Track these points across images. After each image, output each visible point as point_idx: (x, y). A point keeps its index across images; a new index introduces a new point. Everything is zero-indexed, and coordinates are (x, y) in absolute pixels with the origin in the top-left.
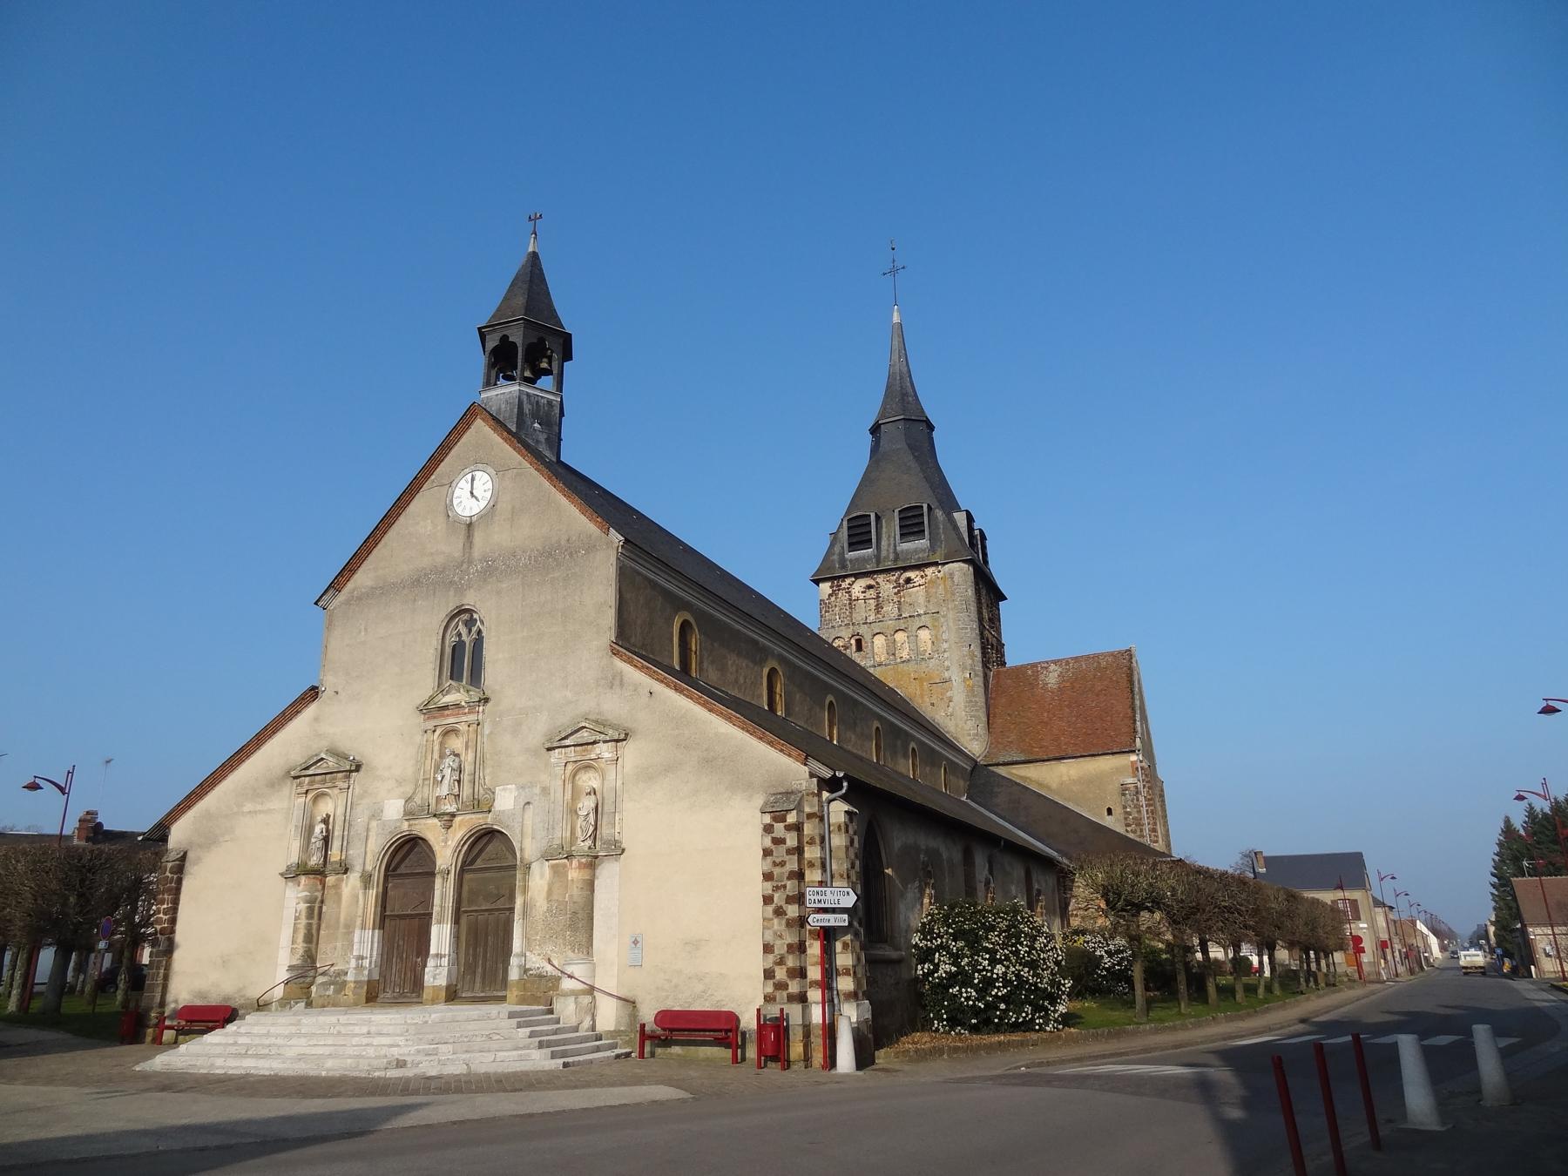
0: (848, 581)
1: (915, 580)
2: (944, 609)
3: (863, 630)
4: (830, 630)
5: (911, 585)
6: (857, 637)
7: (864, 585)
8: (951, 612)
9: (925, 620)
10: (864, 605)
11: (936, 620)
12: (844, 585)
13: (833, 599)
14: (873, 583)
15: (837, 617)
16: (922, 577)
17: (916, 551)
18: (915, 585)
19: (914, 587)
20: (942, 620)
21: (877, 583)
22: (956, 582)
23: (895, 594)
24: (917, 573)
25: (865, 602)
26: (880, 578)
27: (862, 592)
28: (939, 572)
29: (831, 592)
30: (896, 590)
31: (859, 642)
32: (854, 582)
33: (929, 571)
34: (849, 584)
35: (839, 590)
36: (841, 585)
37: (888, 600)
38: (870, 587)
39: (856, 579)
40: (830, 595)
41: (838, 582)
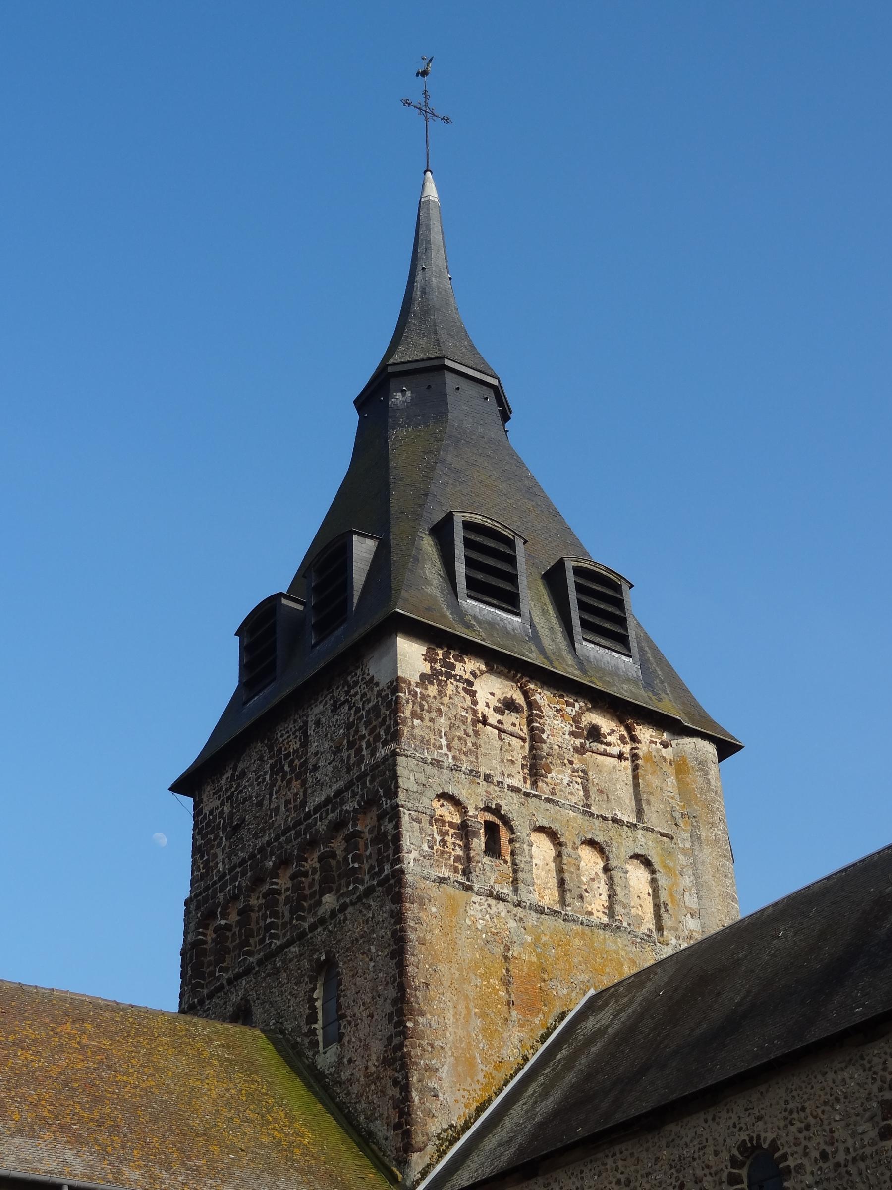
0: (471, 665)
1: (609, 739)
2: (685, 835)
3: (510, 804)
4: (428, 768)
5: (601, 747)
6: (490, 817)
7: (499, 694)
8: (707, 850)
9: (645, 843)
10: (497, 744)
11: (669, 853)
12: (459, 669)
13: (432, 690)
14: (519, 698)
15: (444, 743)
16: (622, 738)
17: (615, 673)
18: (608, 749)
19: (605, 754)
20: (682, 859)
21: (531, 704)
22: (713, 782)
23: (576, 750)
24: (613, 725)
25: (499, 737)
26: (543, 697)
27: (496, 710)
28: (665, 745)
29: (426, 668)
30: (578, 742)
31: (491, 830)
32: (482, 673)
33: (645, 733)
34: (473, 674)
35: (449, 676)
36: (453, 667)
37: (560, 756)
38: (509, 705)
39: (487, 672)
40: (425, 679)
41: (446, 655)
